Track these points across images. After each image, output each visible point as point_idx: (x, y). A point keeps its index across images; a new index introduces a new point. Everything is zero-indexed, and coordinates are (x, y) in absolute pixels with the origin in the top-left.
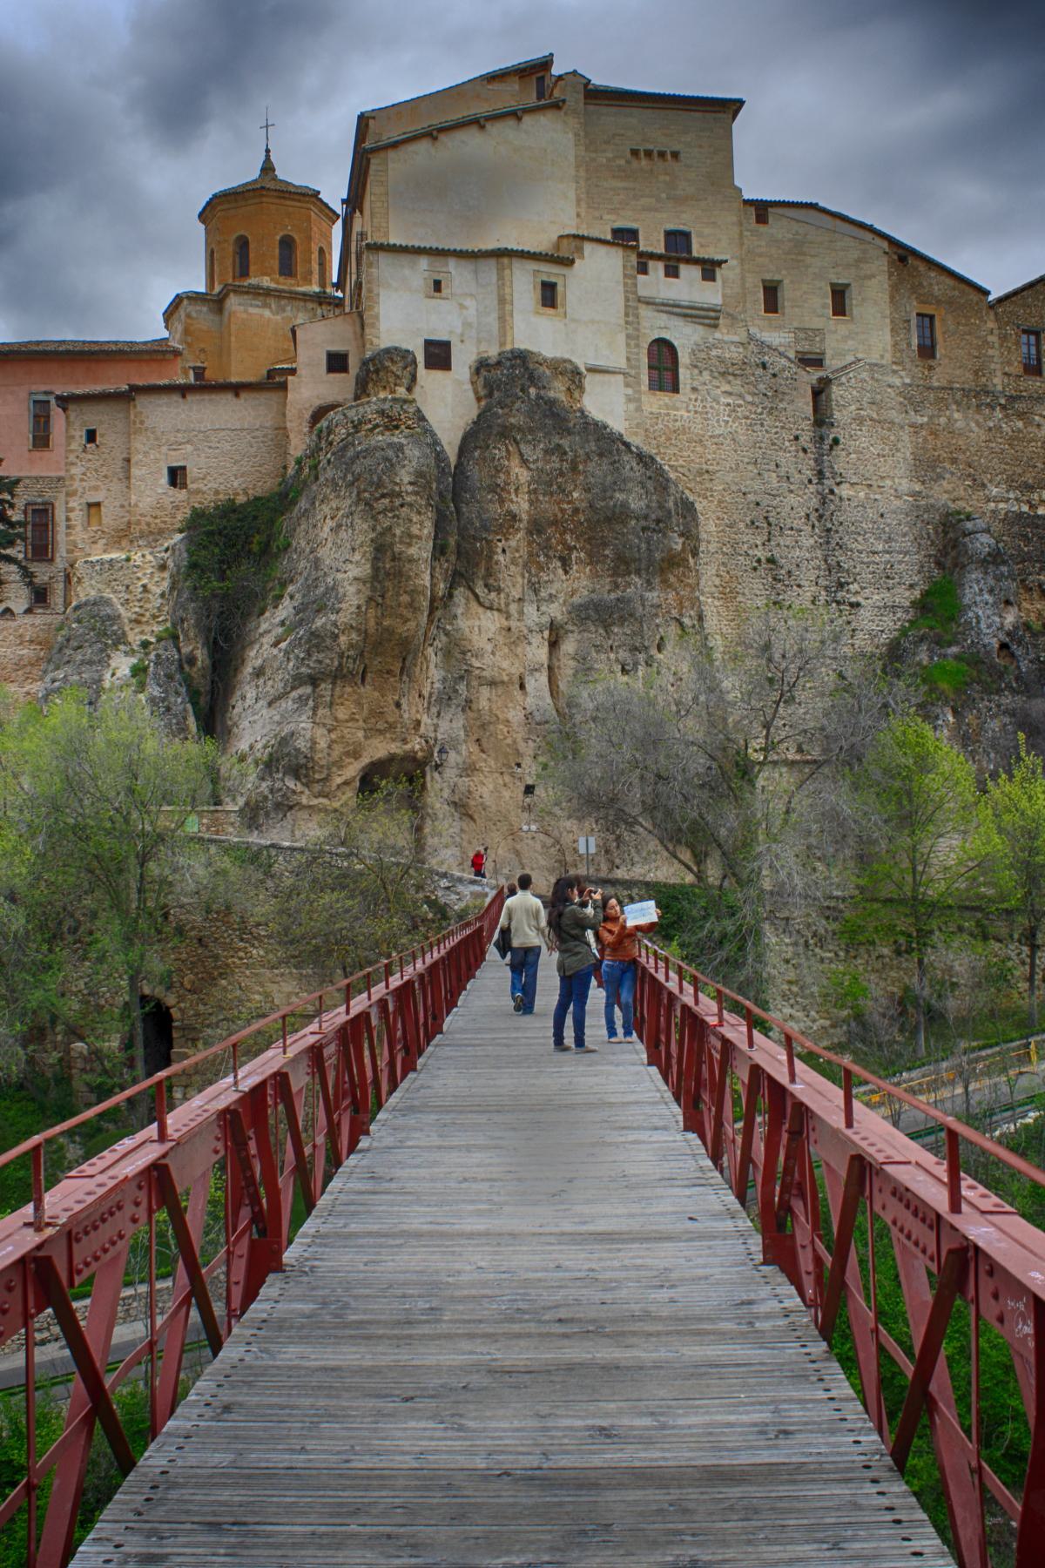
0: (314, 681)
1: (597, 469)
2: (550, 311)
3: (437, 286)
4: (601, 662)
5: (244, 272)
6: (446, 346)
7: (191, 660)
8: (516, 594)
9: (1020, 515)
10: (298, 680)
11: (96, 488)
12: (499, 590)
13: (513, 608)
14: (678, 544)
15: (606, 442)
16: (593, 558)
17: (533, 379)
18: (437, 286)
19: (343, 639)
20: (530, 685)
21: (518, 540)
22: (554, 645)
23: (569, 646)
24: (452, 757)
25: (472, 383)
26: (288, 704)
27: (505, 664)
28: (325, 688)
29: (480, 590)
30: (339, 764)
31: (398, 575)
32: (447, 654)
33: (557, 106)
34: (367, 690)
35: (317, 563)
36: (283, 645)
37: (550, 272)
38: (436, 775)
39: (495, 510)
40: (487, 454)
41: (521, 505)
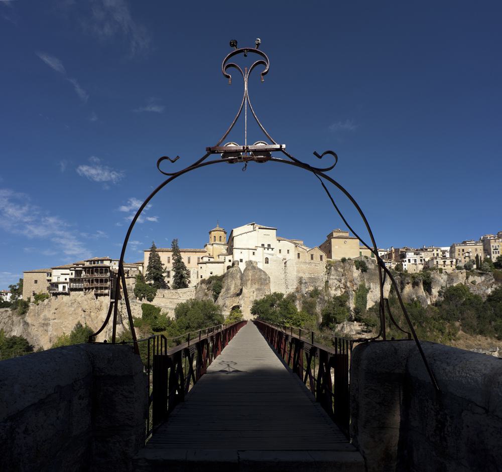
1: (259, 273)
5: (215, 241)
6: (242, 260)
9: (310, 277)
14: (268, 282)
15: (260, 270)
16: (258, 284)
17: (252, 263)
21: (250, 282)
23: (255, 293)
30: (230, 306)
37: (254, 251)
39: (247, 278)
41: (250, 277)
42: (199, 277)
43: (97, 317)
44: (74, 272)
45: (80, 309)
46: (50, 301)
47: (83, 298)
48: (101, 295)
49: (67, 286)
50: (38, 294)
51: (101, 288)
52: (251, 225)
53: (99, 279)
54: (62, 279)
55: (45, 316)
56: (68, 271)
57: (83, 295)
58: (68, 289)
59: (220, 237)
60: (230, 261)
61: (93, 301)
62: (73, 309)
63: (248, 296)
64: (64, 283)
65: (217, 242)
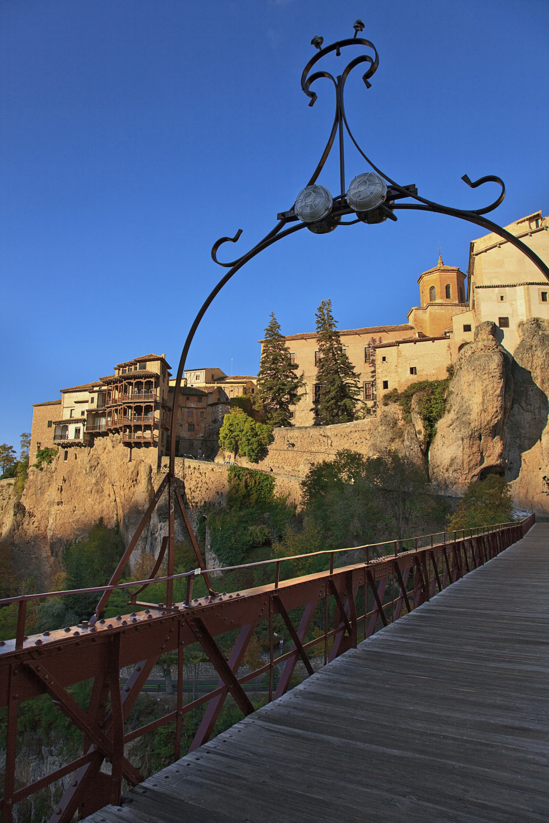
2: (545, 302)
3: (502, 297)
7: (420, 432)
8: (537, 406)
11: (386, 376)
12: (531, 405)
13: (536, 411)
18: (502, 297)
25: (518, 331)
26: (454, 447)
27: (534, 432)
29: (523, 404)
33: (543, 229)
35: (462, 398)
36: (451, 427)
38: (509, 472)
40: (524, 356)
42: (380, 385)
44: (95, 395)
48: (138, 445)
49: (83, 429)
51: (138, 428)
52: (530, 220)
53: (143, 405)
54: (77, 415)
56: (86, 396)
57: (111, 449)
58: (84, 433)
59: (448, 287)
60: (467, 328)
62: (94, 481)
64: (77, 421)
65: (438, 301)
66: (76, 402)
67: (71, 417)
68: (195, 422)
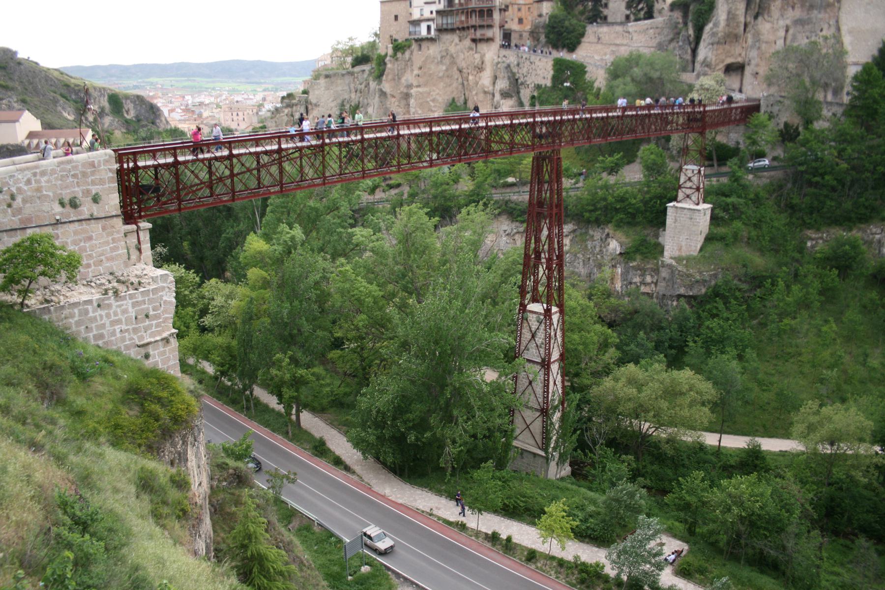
0: (712, 44)
4: (799, 36)
8: (776, 17)
10: (709, 44)
16: (802, 6)
19: (720, 35)
20: (778, 43)
22: (787, 31)
23: (791, 31)
24: (753, 62)
28: (715, 46)
29: (766, 17)
30: (717, 65)
31: (733, 18)
32: (754, 35)
34: (727, 47)
43: (477, 83)
45: (455, 69)
46: (412, 53)
47: (458, 47)
50: (400, 41)
51: (481, 27)
54: (427, 15)
55: (406, 80)
61: (471, 52)
62: (444, 68)
63: (771, 38)
64: (428, 20)
66: (426, 3)
67: (422, 15)
68: (523, 17)
